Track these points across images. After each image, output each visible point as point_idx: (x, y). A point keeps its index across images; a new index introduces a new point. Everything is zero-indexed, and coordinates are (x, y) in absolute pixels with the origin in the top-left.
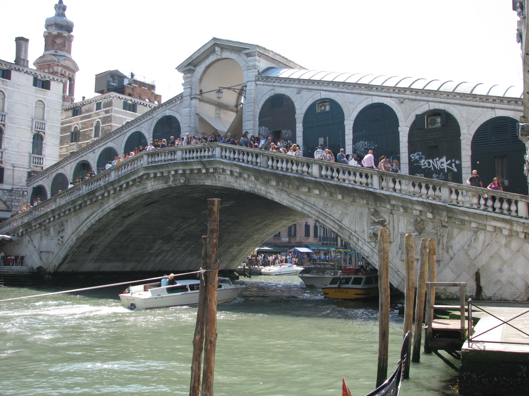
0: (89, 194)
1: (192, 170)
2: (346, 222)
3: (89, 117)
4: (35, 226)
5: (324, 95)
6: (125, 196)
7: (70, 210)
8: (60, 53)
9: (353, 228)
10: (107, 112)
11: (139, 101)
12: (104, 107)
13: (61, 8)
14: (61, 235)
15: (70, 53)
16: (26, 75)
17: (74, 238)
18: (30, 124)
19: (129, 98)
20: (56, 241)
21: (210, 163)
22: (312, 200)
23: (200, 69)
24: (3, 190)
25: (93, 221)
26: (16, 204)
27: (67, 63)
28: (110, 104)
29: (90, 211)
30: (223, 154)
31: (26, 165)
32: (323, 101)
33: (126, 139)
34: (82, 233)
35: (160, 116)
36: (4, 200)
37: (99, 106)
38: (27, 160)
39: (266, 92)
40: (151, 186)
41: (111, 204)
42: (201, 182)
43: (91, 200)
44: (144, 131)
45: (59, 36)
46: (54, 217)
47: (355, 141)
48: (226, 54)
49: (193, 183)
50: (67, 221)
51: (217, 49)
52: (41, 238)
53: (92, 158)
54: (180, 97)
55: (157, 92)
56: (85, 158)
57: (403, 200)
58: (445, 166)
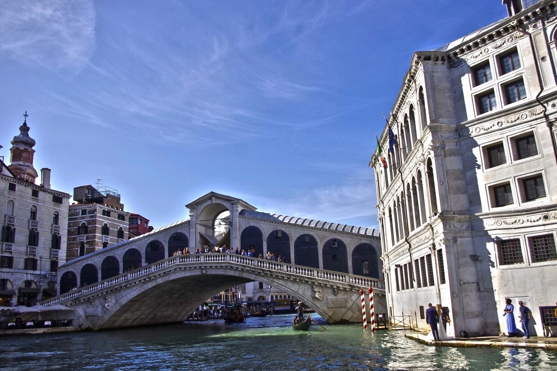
1: (211, 267)
2: (300, 292)
3: (76, 219)
4: (84, 300)
6: (160, 281)
7: (116, 289)
8: (26, 164)
10: (91, 217)
11: (112, 209)
12: (89, 213)
13: (25, 129)
14: (106, 305)
15: (32, 163)
18: (50, 228)
19: (107, 207)
24: (35, 274)
26: (42, 284)
27: (30, 171)
30: (231, 258)
31: (48, 256)
36: (35, 281)
37: (84, 212)
38: (48, 252)
44: (160, 240)
45: (26, 150)
51: (213, 198)
53: (119, 255)
54: (188, 222)
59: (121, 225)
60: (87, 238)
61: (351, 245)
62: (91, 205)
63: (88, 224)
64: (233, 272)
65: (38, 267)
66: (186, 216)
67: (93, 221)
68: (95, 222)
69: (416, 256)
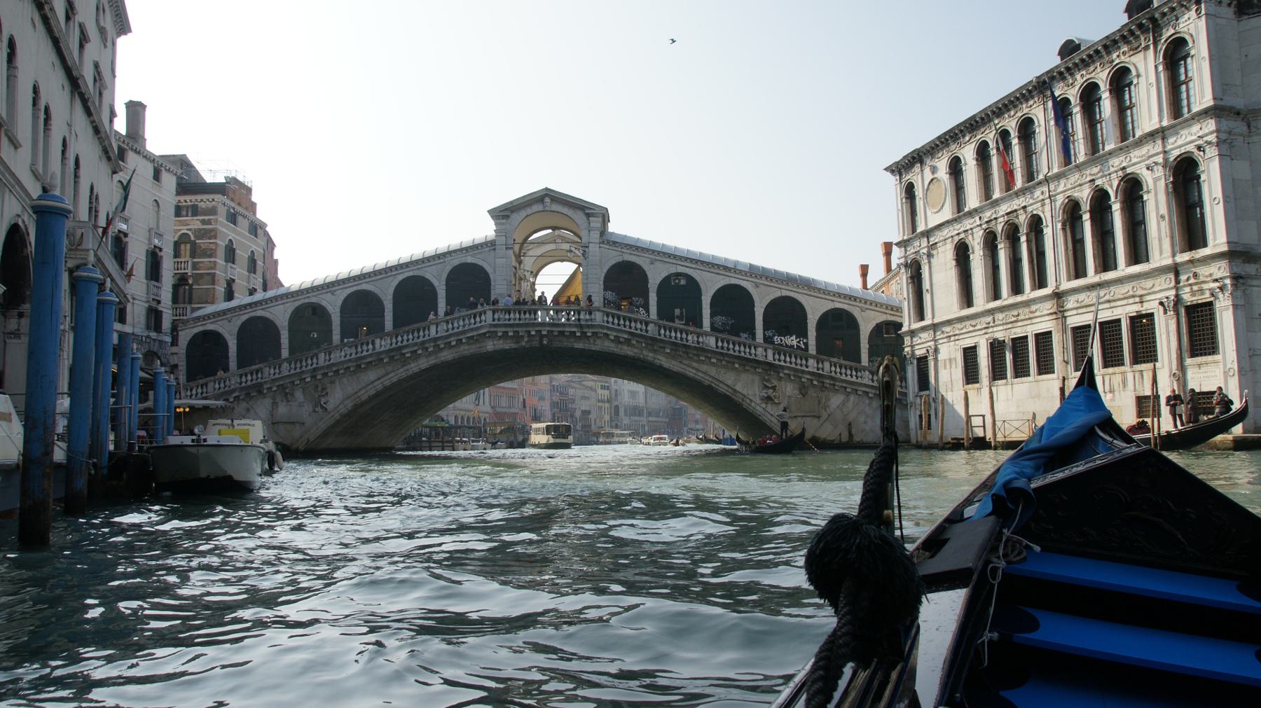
0: (390, 351)
2: (738, 388)
4: (270, 389)
5: (681, 270)
6: (447, 355)
9: (745, 392)
10: (203, 222)
16: (144, 160)
17: (350, 404)
20: (308, 408)
21: (588, 326)
22: (704, 368)
23: (517, 217)
25: (387, 383)
28: (213, 211)
29: (381, 372)
32: (678, 275)
33: (396, 282)
34: (364, 398)
35: (456, 262)
38: (145, 286)
39: (614, 257)
40: (490, 346)
41: (424, 363)
42: (570, 345)
43: (392, 358)
44: (428, 276)
46: (314, 377)
47: (712, 315)
48: (556, 207)
49: (556, 344)
50: (332, 382)
51: (547, 200)
52: (275, 404)
54: (489, 245)
55: (254, 199)
56: (314, 300)
57: (795, 370)
58: (795, 343)
59: (254, 247)
60: (195, 266)
61: (814, 310)
62: (205, 197)
63: (197, 237)
64: (607, 343)
65: (129, 318)
66: (486, 229)
67: (212, 230)
68: (212, 234)
69: (1075, 320)
